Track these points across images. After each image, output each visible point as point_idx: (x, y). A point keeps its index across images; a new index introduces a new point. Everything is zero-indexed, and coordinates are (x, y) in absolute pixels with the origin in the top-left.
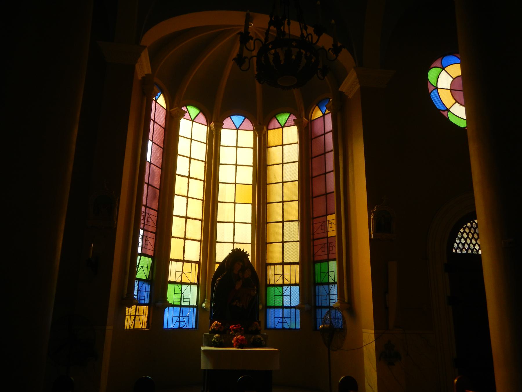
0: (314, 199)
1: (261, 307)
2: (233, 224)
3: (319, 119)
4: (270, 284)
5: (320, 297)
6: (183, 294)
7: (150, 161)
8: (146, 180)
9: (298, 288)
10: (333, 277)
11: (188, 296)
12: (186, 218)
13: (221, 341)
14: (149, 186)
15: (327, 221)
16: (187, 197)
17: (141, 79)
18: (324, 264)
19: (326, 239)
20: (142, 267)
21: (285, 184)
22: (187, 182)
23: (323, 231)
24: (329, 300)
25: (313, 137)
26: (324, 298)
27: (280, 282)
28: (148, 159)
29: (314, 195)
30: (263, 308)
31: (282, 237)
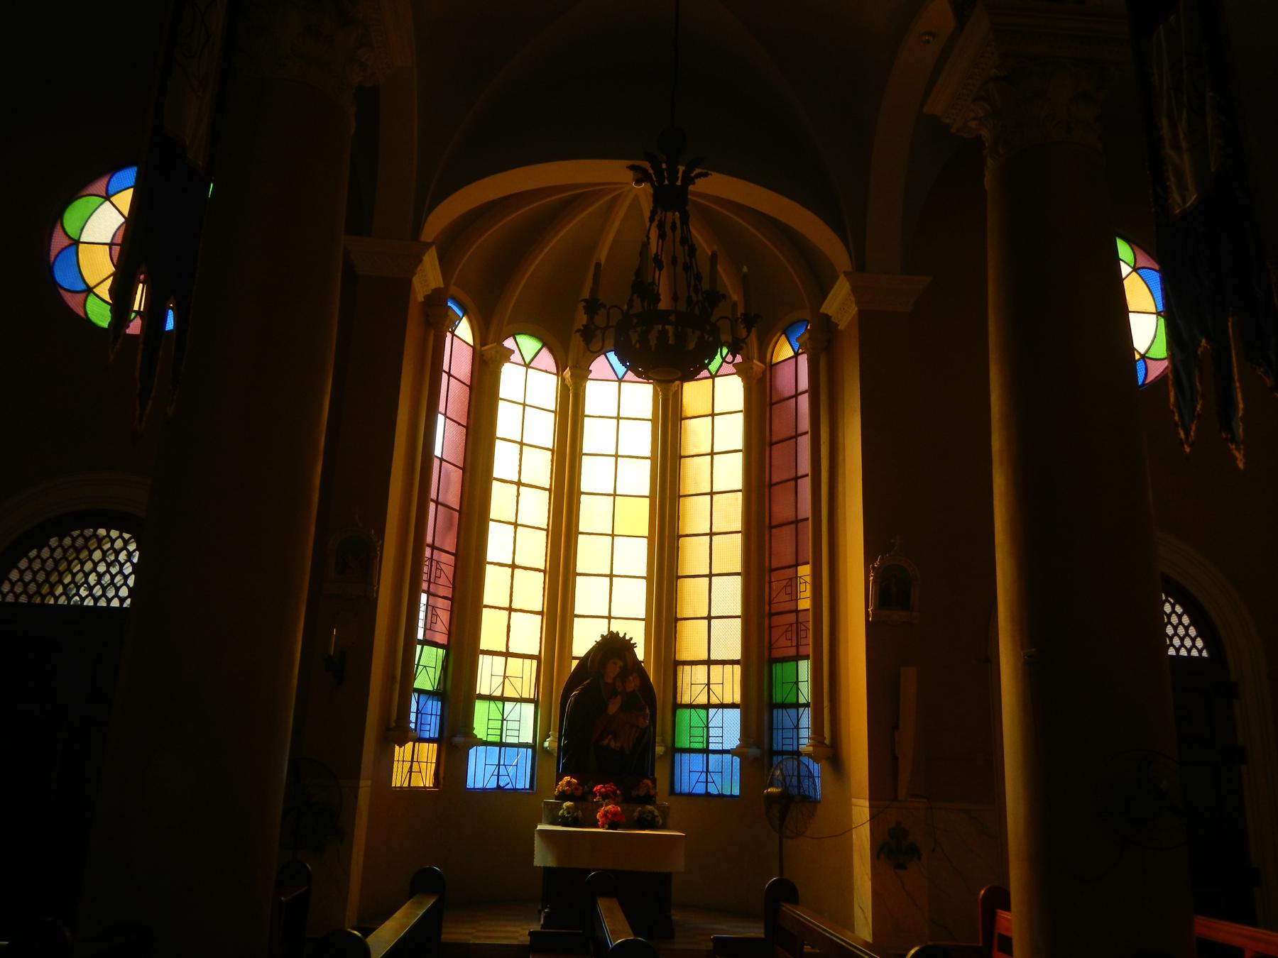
0: (774, 531)
1: (659, 750)
2: (608, 579)
4: (683, 702)
5: (780, 731)
8: (433, 495)
10: (805, 693)
11: (516, 725)
12: (513, 566)
13: (575, 814)
14: (439, 506)
15: (797, 577)
16: (516, 525)
17: (423, 300)
19: (794, 614)
20: (425, 666)
23: (788, 598)
24: (798, 738)
25: (775, 399)
26: (788, 734)
27: (703, 700)
28: (438, 452)
29: (774, 523)
30: (666, 752)
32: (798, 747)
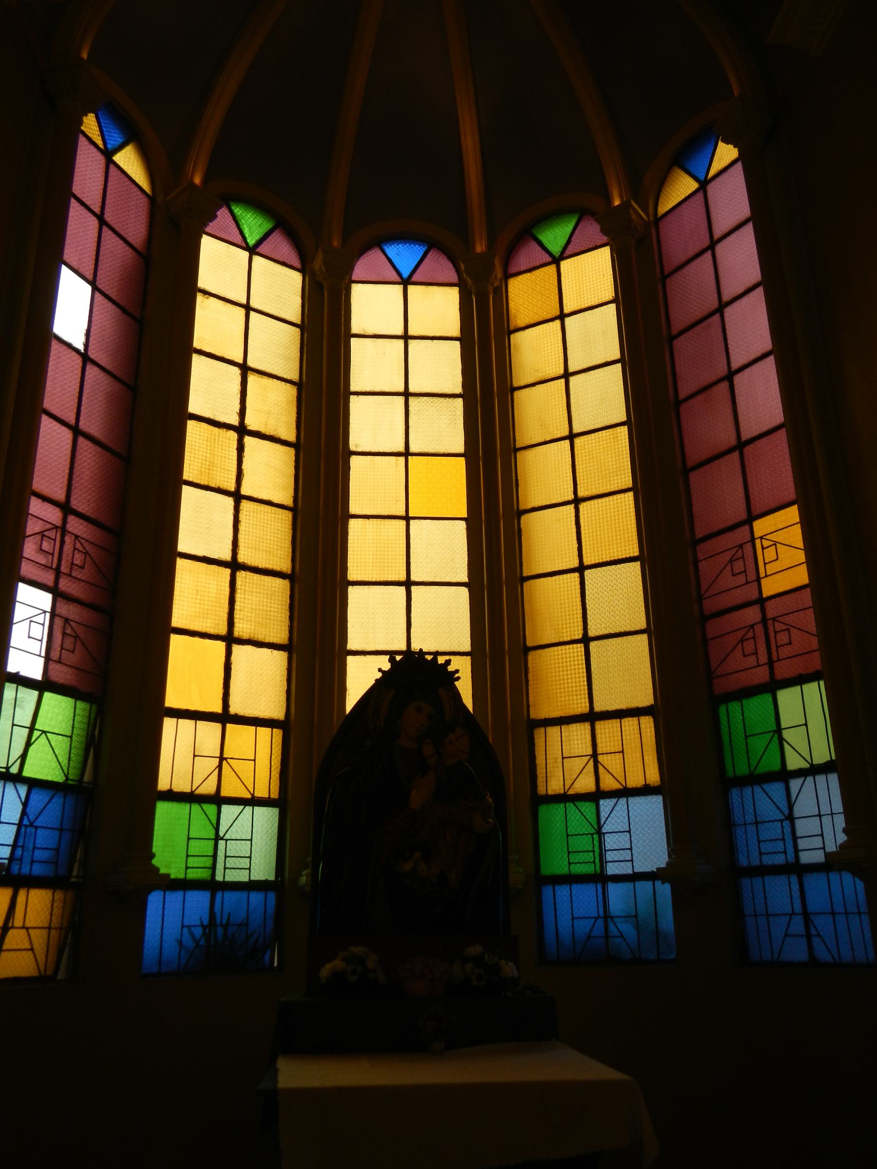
3: (684, 205)
4: (550, 792)
5: (751, 829)
6: (222, 839)
9: (656, 802)
11: (243, 848)
12: (234, 566)
14: (81, 440)
15: (753, 540)
18: (758, 705)
20: (44, 732)
21: (578, 441)
24: (795, 838)
25: (667, 269)
27: (586, 784)
29: (690, 463)
31: (581, 624)
32: (797, 857)
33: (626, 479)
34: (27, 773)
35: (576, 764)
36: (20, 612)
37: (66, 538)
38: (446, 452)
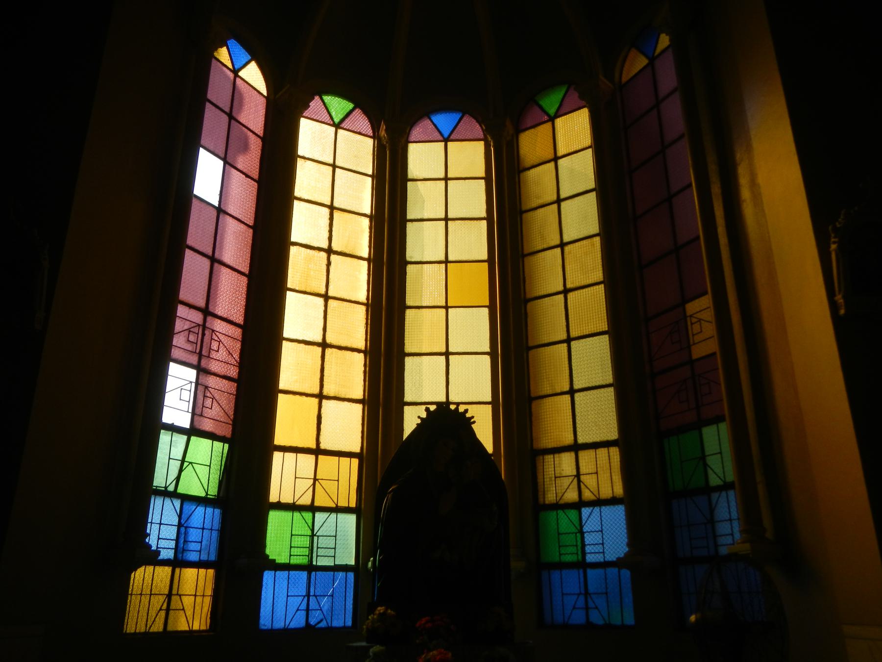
1: (517, 565)
4: (547, 502)
7: (216, 204)
9: (619, 511)
10: (719, 470)
11: (330, 542)
15: (685, 316)
20: (191, 463)
22: (325, 262)
24: (715, 536)
27: (572, 496)
33: (598, 275)
34: (181, 490)
35: (566, 482)
36: (171, 383)
37: (206, 332)
38: (474, 259)
